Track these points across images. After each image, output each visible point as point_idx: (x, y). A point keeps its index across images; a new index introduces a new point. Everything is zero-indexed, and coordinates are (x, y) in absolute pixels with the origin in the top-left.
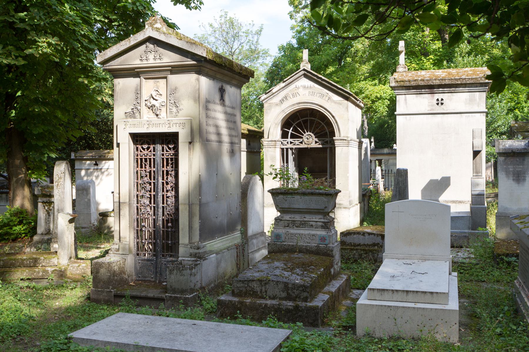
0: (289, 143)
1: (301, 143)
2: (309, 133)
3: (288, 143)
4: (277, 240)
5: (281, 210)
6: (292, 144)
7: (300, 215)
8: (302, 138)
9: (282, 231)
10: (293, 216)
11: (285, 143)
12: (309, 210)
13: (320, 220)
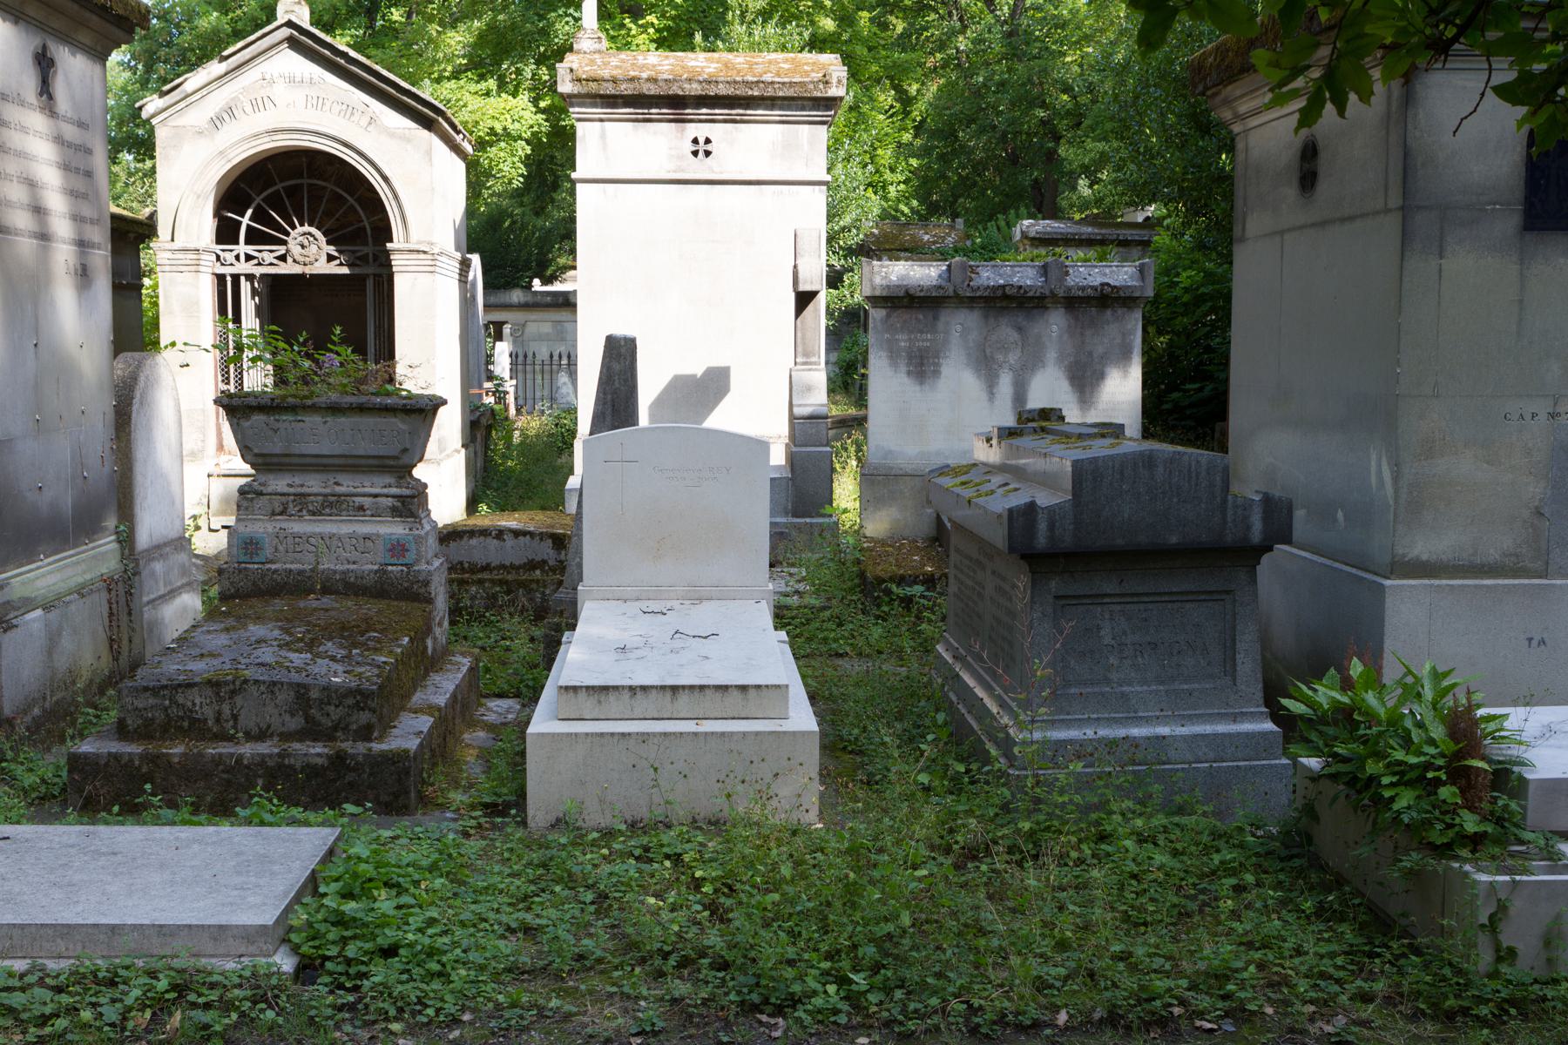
0: (242, 258)
1: (283, 258)
2: (307, 228)
3: (237, 258)
4: (247, 559)
5: (260, 460)
7: (323, 477)
8: (284, 243)
9: (263, 528)
10: (297, 480)
11: (230, 257)
12: (350, 461)
13: (385, 491)
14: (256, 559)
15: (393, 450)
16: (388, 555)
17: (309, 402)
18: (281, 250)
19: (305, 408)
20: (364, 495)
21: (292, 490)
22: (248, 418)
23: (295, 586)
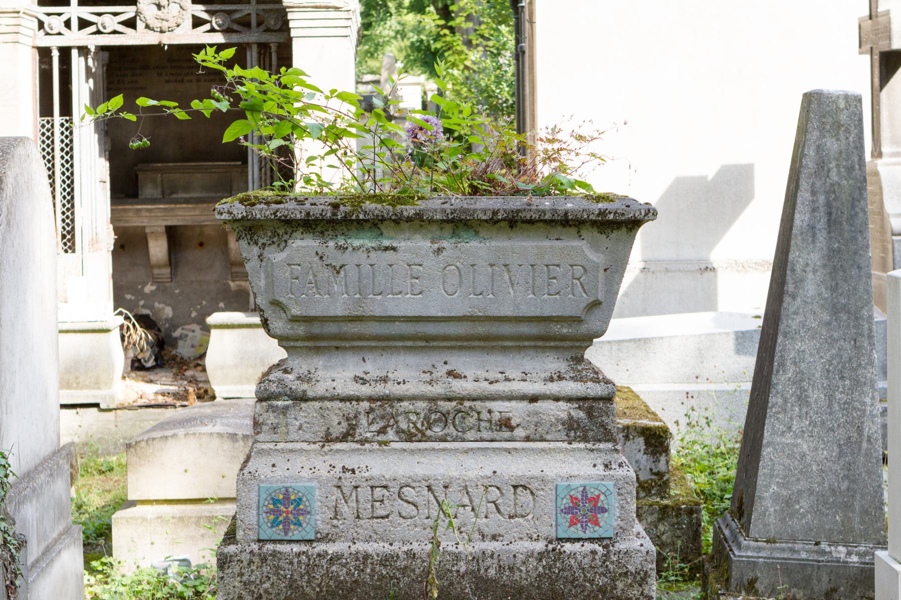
0: (75, 24)
1: (131, 23)
3: (68, 24)
4: (277, 533)
5: (301, 330)
9: (304, 468)
10: (373, 366)
11: (57, 23)
12: (481, 329)
13: (554, 388)
14: (296, 534)
16: (565, 520)
17: (409, 210)
19: (398, 221)
20: (510, 398)
21: (365, 390)
22: (282, 244)
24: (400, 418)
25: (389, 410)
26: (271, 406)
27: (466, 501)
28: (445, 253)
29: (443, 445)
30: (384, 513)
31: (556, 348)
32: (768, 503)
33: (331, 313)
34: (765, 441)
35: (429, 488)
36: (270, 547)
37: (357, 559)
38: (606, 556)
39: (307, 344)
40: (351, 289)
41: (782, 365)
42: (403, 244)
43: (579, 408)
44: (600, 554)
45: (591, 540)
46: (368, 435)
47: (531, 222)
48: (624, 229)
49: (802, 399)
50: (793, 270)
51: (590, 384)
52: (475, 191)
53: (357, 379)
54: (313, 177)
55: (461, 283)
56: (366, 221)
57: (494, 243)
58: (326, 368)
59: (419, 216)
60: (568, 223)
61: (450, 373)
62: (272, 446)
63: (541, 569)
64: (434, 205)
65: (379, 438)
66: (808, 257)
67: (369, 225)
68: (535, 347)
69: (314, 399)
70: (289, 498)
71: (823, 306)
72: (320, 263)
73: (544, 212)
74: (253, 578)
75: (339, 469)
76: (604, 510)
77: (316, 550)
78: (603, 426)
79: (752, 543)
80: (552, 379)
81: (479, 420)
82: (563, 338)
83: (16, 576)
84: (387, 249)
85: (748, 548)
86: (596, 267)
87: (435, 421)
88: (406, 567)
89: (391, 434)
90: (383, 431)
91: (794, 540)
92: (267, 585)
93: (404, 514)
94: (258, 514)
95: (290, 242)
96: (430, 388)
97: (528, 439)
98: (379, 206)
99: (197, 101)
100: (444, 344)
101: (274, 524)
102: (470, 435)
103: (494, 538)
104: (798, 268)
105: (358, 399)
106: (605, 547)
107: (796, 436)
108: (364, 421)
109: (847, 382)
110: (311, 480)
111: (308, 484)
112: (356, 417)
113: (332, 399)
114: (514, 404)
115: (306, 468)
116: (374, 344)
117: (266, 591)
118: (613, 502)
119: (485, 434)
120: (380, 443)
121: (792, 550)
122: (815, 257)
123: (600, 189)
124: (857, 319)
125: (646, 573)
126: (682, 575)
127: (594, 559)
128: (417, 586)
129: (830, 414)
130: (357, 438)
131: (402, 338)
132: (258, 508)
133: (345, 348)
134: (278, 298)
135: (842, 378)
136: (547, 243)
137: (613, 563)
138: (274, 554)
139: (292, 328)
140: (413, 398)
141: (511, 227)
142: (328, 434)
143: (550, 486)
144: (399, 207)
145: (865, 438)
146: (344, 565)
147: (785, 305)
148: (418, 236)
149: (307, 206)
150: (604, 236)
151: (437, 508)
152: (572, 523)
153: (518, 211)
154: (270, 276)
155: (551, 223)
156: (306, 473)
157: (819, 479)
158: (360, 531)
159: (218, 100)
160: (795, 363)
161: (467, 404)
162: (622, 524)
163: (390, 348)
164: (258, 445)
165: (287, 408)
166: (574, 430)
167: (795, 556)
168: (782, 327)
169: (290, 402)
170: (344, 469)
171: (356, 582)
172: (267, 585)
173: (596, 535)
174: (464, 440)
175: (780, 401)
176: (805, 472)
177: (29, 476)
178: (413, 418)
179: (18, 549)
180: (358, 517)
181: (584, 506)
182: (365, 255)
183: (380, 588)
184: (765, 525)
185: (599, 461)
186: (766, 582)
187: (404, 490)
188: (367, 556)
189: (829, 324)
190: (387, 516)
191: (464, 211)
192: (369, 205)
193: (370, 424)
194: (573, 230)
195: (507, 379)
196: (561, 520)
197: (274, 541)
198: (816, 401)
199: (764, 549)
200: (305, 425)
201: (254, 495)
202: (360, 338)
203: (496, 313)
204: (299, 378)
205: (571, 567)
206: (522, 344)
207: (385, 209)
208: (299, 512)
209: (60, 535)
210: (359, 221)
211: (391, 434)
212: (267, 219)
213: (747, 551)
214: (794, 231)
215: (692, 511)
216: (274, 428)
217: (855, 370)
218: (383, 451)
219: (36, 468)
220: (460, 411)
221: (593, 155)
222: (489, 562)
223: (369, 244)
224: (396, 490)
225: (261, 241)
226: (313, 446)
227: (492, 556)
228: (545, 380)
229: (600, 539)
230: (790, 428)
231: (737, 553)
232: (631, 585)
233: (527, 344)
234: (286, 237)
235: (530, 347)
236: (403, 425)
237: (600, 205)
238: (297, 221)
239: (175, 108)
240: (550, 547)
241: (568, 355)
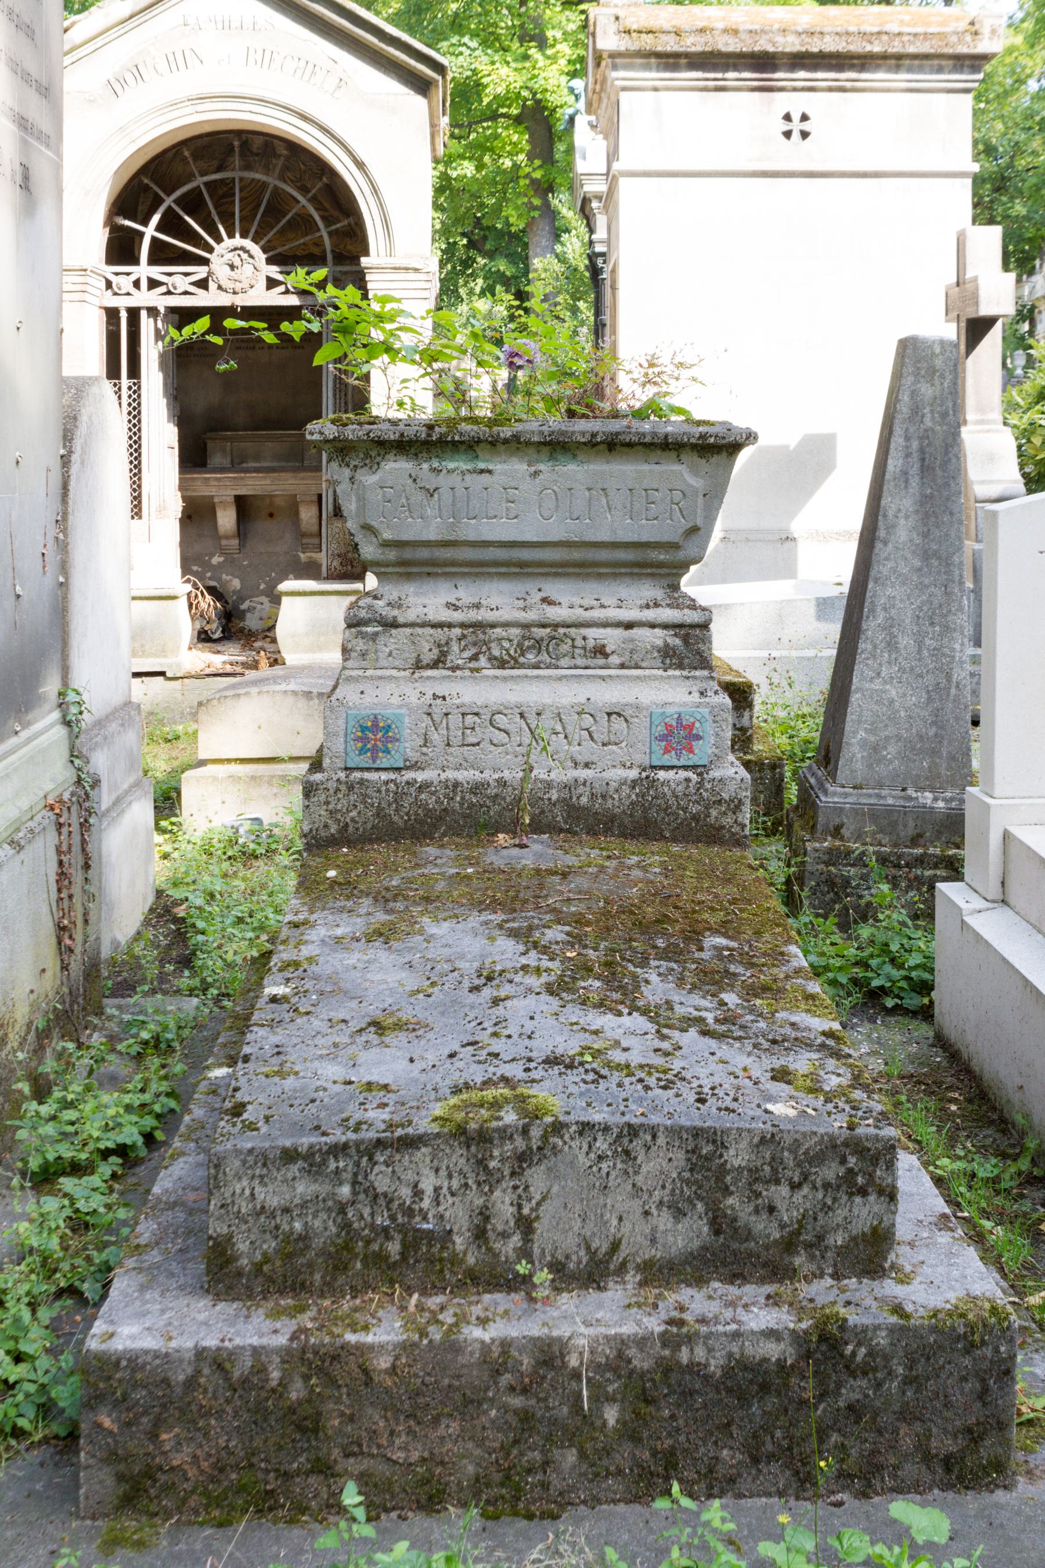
0: (144, 284)
1: (203, 284)
2: (238, 241)
3: (137, 284)
4: (365, 761)
5: (392, 555)
6: (152, 288)
7: (518, 587)
8: (205, 262)
9: (395, 695)
10: (466, 592)
11: (125, 283)
12: (576, 555)
13: (650, 615)
14: (384, 762)
15: (667, 530)
17: (506, 432)
18: (201, 272)
19: (494, 443)
20: (605, 625)
21: (457, 616)
22: (373, 465)
23: (472, 818)
24: (492, 645)
25: (481, 636)
26: (361, 633)
27: (559, 728)
28: (541, 476)
29: (536, 672)
30: (475, 740)
31: (652, 575)
32: (855, 749)
33: (424, 538)
34: (853, 687)
35: (522, 715)
36: (357, 775)
37: (447, 787)
38: (700, 784)
39: (397, 570)
40: (445, 514)
41: (872, 610)
42: (499, 467)
43: (675, 635)
44: (694, 782)
45: (685, 768)
46: (460, 662)
47: (630, 445)
48: (724, 454)
49: (892, 645)
50: (885, 516)
51: (686, 611)
52: (571, 414)
53: (449, 605)
54: (407, 400)
55: (557, 508)
56: (462, 442)
57: (592, 467)
58: (416, 594)
59: (516, 437)
60: (668, 446)
61: (544, 600)
62: (360, 673)
63: (634, 797)
64: (531, 427)
65: (471, 665)
66: (900, 504)
67: (463, 448)
68: (631, 574)
69: (405, 625)
70: (377, 726)
71: (914, 552)
72: (413, 485)
73: (644, 435)
74: (339, 807)
75: (429, 695)
76: (698, 738)
77: (405, 778)
78: (699, 653)
79: (839, 790)
80: (648, 606)
81: (574, 647)
82: (661, 565)
83: (90, 814)
84: (482, 471)
85: (835, 794)
86: (696, 491)
87: (529, 648)
88: (496, 795)
89: (483, 661)
90: (475, 658)
91: (880, 786)
92: (354, 814)
93: (495, 741)
94: (346, 742)
95: (383, 464)
96: (523, 614)
97: (622, 666)
98: (475, 428)
99: (286, 323)
100: (539, 570)
101: (362, 751)
102: (563, 662)
103: (587, 765)
104: (890, 513)
105: (450, 626)
106: (700, 774)
107: (885, 682)
108: (455, 648)
109: (937, 628)
110: (400, 707)
111: (398, 711)
112: (447, 643)
113: (423, 625)
114: (609, 630)
115: (396, 695)
116: (466, 570)
117: (353, 820)
118: (708, 730)
119: (579, 661)
120: (472, 670)
121: (879, 796)
122: (908, 503)
123: (697, 416)
124: (948, 565)
125: (740, 801)
126: (764, 829)
127: (688, 787)
128: (507, 814)
129: (920, 660)
130: (449, 665)
131: (496, 564)
132: (346, 735)
133: (436, 575)
134: (369, 521)
135: (932, 624)
136: (646, 467)
137: (706, 790)
138: (362, 782)
139: (383, 553)
140: (506, 625)
141: (610, 450)
142: (418, 660)
143: (645, 713)
144: (495, 429)
145: (954, 685)
146: (433, 793)
147: (876, 550)
148: (514, 459)
149: (402, 427)
150: (704, 461)
151: (529, 735)
152: (667, 751)
153: (618, 434)
154: (362, 500)
155: (650, 446)
156: (395, 700)
157: (907, 726)
158: (451, 759)
159: (309, 321)
160: (885, 609)
161: (561, 631)
162: (716, 751)
163: (482, 574)
164: (347, 673)
165: (376, 634)
166: (669, 657)
167: (882, 802)
168: (873, 573)
169: (380, 628)
170: (435, 696)
171: (445, 810)
172: (354, 814)
173: (690, 763)
174: (557, 667)
175: (870, 647)
176: (893, 719)
177: (100, 724)
178: (506, 644)
179: (92, 787)
180: (448, 745)
181: (679, 734)
182: (460, 478)
183: (469, 816)
184: (852, 772)
185: (695, 689)
186: (852, 827)
187: (496, 717)
188: (456, 784)
189: (920, 570)
190: (478, 744)
191: (563, 433)
192: (464, 427)
193: (461, 651)
194: (673, 454)
195: (602, 606)
196: (655, 747)
197: (362, 769)
198: (905, 647)
199: (851, 795)
200: (394, 652)
201: (341, 722)
202: (453, 563)
203: (593, 539)
204: (389, 604)
205: (664, 794)
206: (617, 571)
207: (483, 430)
208: (387, 740)
209: (131, 787)
210: (454, 443)
211: (483, 661)
212: (360, 440)
213: (834, 797)
214: (887, 477)
215: (775, 766)
216: (363, 655)
217: (945, 616)
218: (475, 678)
219: (107, 717)
220: (554, 638)
221: (694, 379)
222: (581, 789)
223: (464, 466)
224: (488, 717)
225: (353, 463)
226: (402, 673)
227: (584, 784)
228: (641, 607)
229: (694, 767)
230: (879, 674)
231: (823, 799)
232: (725, 813)
233: (623, 570)
234: (378, 459)
235: (626, 574)
236: (496, 652)
237: (701, 429)
238: (390, 442)
239: (264, 329)
240: (644, 774)
241: (665, 582)
